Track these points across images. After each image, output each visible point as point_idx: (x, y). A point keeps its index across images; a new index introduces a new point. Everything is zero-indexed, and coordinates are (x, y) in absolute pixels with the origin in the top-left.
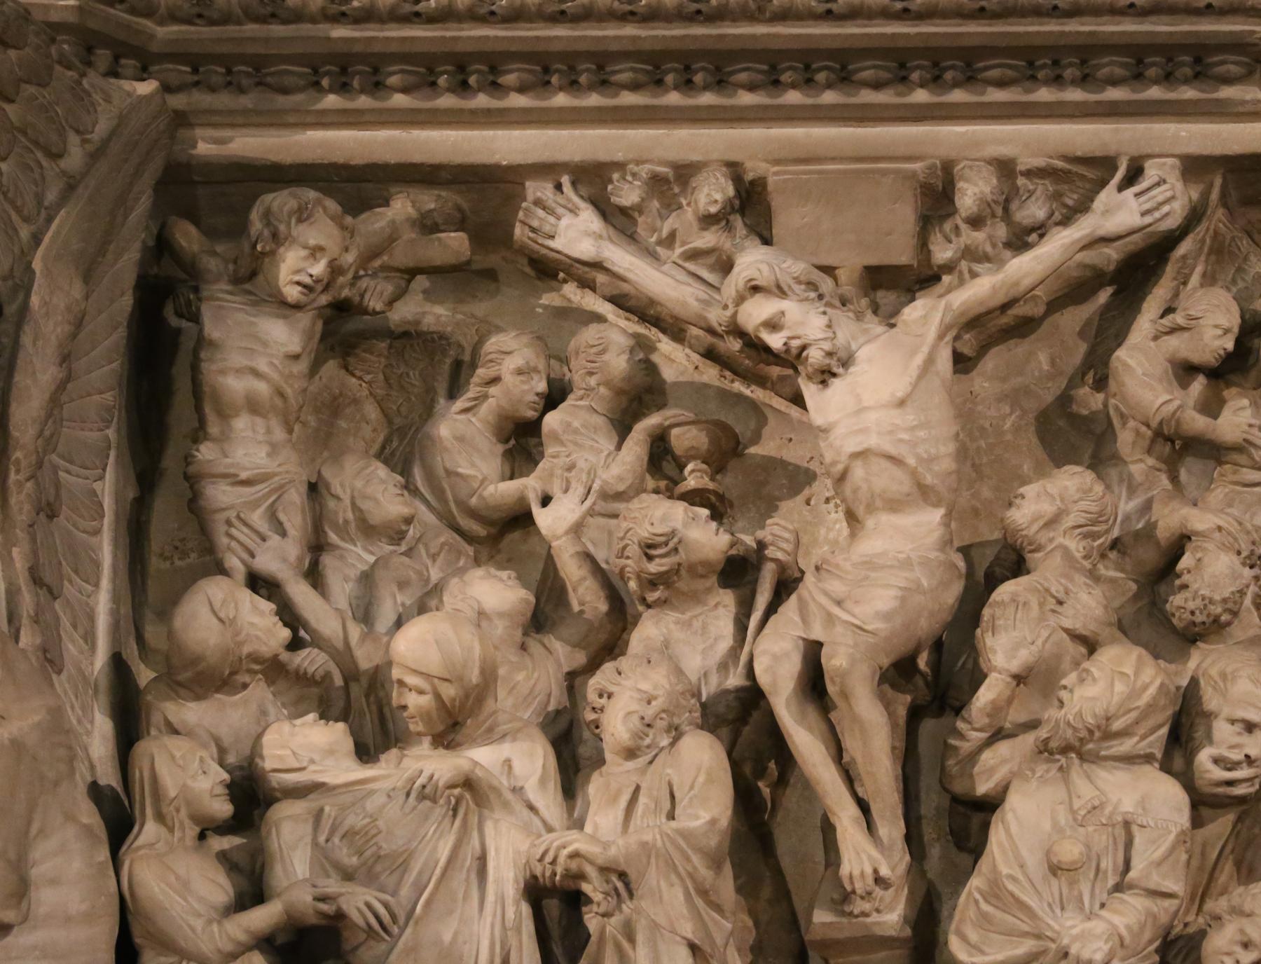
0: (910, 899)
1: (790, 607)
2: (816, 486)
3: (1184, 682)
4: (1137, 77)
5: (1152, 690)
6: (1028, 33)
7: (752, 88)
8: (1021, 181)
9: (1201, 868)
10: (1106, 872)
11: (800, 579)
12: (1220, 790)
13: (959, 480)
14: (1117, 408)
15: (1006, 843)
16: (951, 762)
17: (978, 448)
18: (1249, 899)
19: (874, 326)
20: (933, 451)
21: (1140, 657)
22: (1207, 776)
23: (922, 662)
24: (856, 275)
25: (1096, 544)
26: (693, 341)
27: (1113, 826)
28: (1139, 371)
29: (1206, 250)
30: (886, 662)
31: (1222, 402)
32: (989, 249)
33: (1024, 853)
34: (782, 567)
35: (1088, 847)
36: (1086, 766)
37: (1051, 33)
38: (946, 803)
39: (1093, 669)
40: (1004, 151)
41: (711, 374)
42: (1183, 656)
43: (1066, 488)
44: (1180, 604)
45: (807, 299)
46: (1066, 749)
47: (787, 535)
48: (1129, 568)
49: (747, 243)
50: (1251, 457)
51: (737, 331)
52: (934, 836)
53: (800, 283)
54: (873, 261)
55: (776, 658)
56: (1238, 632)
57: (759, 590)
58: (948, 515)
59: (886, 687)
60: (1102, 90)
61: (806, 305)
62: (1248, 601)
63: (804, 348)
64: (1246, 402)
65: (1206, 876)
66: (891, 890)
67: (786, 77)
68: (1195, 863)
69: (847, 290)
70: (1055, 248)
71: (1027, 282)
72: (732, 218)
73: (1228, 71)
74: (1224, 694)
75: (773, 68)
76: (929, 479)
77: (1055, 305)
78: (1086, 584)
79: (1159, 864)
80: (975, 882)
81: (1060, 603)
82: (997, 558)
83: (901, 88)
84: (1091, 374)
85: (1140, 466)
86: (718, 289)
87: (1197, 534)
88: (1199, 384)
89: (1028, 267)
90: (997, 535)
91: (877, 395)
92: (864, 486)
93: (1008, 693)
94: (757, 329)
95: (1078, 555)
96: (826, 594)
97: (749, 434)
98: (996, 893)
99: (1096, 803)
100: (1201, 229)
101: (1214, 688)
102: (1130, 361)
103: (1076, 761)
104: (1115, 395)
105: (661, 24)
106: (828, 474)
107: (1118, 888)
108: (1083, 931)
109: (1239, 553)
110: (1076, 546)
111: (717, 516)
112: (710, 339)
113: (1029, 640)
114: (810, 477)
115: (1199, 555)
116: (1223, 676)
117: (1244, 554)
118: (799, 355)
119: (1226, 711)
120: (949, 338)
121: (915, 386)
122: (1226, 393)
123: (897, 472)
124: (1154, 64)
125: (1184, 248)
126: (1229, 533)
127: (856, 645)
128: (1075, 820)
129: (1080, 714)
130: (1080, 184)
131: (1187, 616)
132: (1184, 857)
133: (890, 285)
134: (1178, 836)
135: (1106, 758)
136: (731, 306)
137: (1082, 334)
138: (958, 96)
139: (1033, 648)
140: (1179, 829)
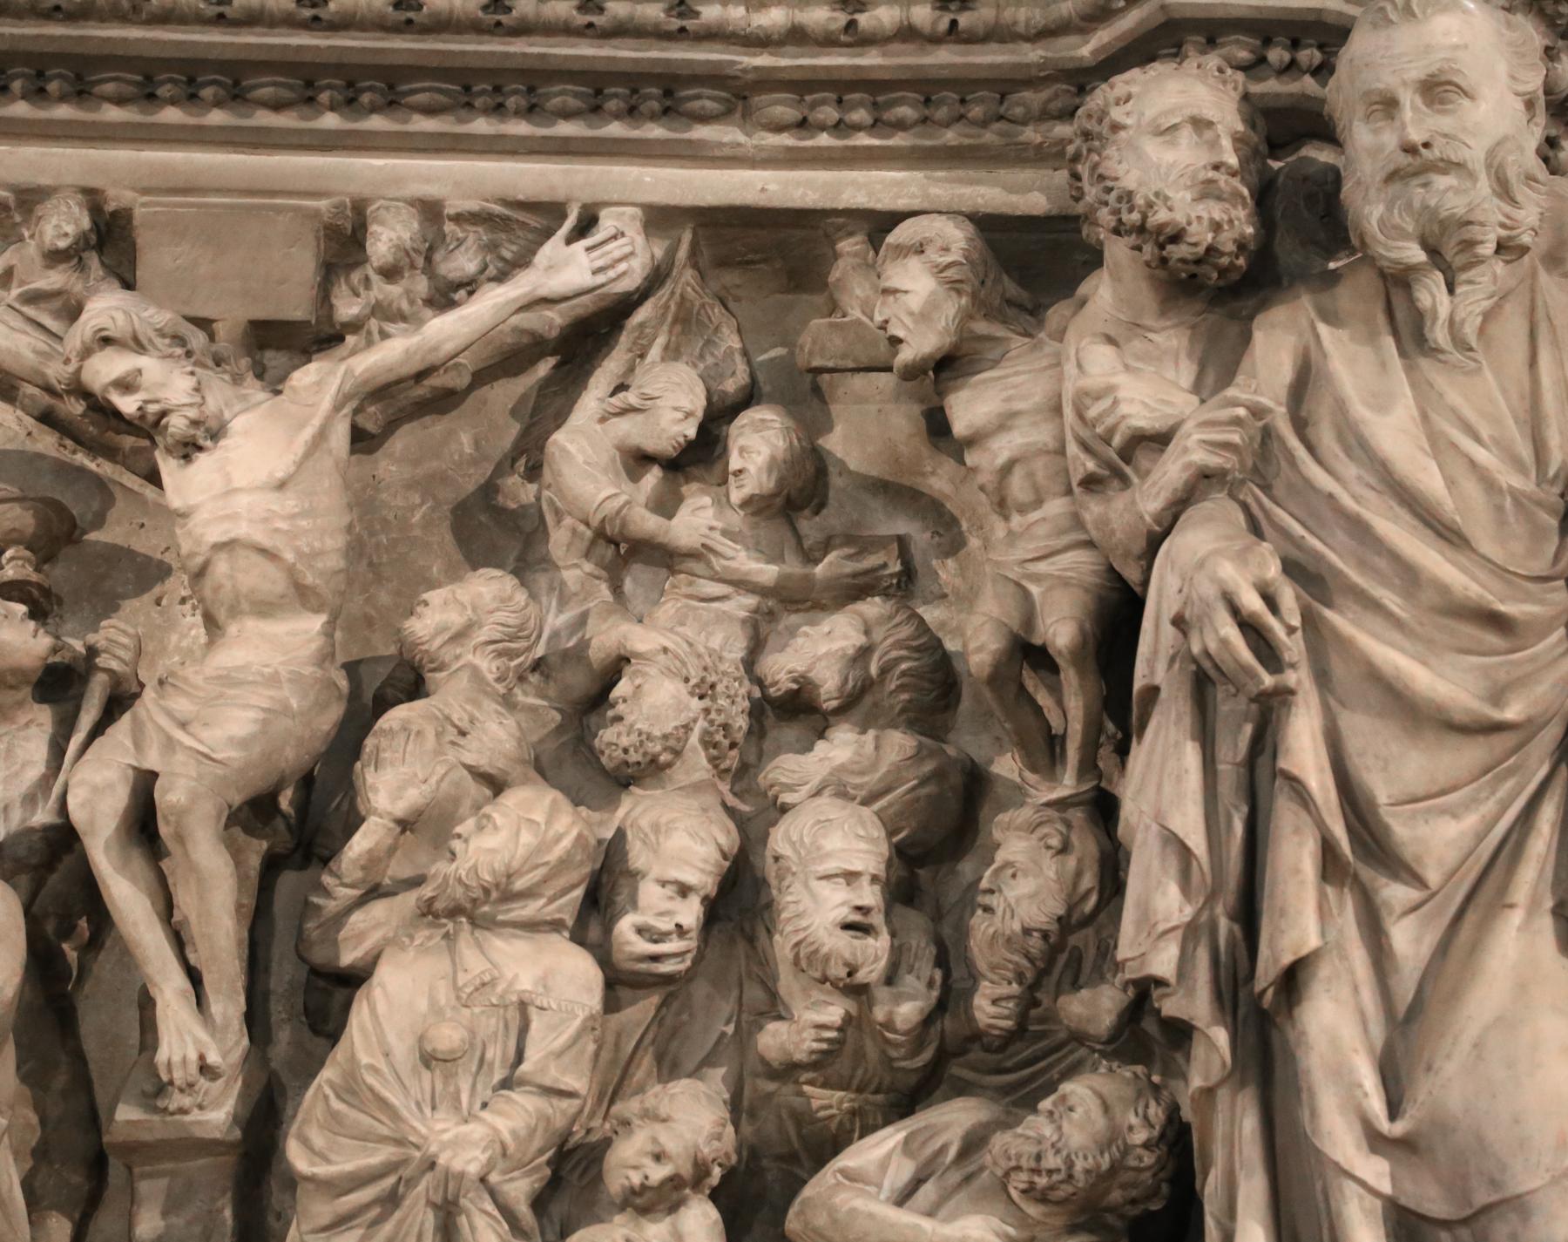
0: (243, 1096)
1: (121, 729)
2: (170, 583)
3: (609, 834)
4: (595, 110)
5: (566, 843)
6: (463, 53)
7: (120, 101)
8: (449, 227)
9: (613, 1062)
10: (491, 1064)
11: (137, 696)
12: (643, 966)
13: (350, 582)
14: (551, 502)
15: (369, 1026)
16: (310, 925)
17: (378, 545)
18: (666, 1100)
19: (255, 391)
20: (317, 544)
21: (554, 801)
22: (628, 948)
23: (285, 801)
24: (240, 330)
25: (513, 664)
26: (26, 401)
27: (506, 1007)
28: (580, 459)
29: (670, 319)
30: (237, 799)
31: (679, 499)
32: (405, 306)
33: (392, 1038)
34: (116, 679)
35: (472, 1033)
36: (478, 933)
37: (492, 53)
38: (303, 973)
39: (495, 815)
41: (47, 443)
42: (611, 803)
43: (480, 595)
44: (613, 739)
45: (171, 356)
46: (454, 912)
47: (125, 640)
48: (552, 693)
49: (104, 286)
50: (709, 564)
51: (80, 390)
52: (284, 1016)
53: (163, 336)
54: (261, 314)
55: (95, 789)
56: (681, 775)
57: (84, 707)
58: (331, 625)
59: (237, 831)
60: (553, 124)
61: (169, 363)
62: (694, 739)
63: (164, 414)
64: (707, 500)
65: (619, 1072)
66: (220, 1082)
67: (164, 91)
68: (605, 1055)
69: (222, 346)
70: (487, 308)
71: (449, 347)
72: (85, 255)
73: (703, 108)
75: (149, 78)
76: (309, 579)
77: (483, 377)
78: (497, 712)
79: (559, 1054)
80: (327, 1074)
81: (463, 734)
82: (390, 677)
83: (306, 110)
84: (523, 461)
85: (575, 572)
86: (59, 338)
87: (638, 655)
88: (653, 477)
89: (449, 330)
90: (392, 650)
91: (252, 476)
92: (228, 585)
93: (390, 841)
94: (105, 388)
95: (490, 677)
96: (169, 714)
97: (89, 516)
98: (351, 1089)
99: (487, 978)
100: (663, 294)
101: (644, 842)
102: (572, 448)
103: (466, 927)
104: (549, 486)
105: (9, 20)
106: (183, 568)
107: (506, 1084)
108: (456, 1137)
109: (687, 680)
110: (488, 666)
111: (38, 613)
112: (47, 399)
113: (421, 776)
114: (164, 571)
115: (637, 682)
116: (656, 828)
117: (693, 681)
118: (157, 423)
119: (656, 871)
120: (347, 410)
121: (300, 465)
122: (684, 489)
123: (271, 569)
124: (616, 95)
125: (642, 314)
126: (677, 657)
127: (200, 777)
128: (458, 998)
129: (475, 868)
130: (520, 233)
131: (619, 753)
132: (591, 1047)
133: (277, 344)
134: (585, 1020)
135: (505, 924)
136: (74, 360)
137: (514, 413)
138: (377, 123)
139: (424, 787)
140: (587, 1013)
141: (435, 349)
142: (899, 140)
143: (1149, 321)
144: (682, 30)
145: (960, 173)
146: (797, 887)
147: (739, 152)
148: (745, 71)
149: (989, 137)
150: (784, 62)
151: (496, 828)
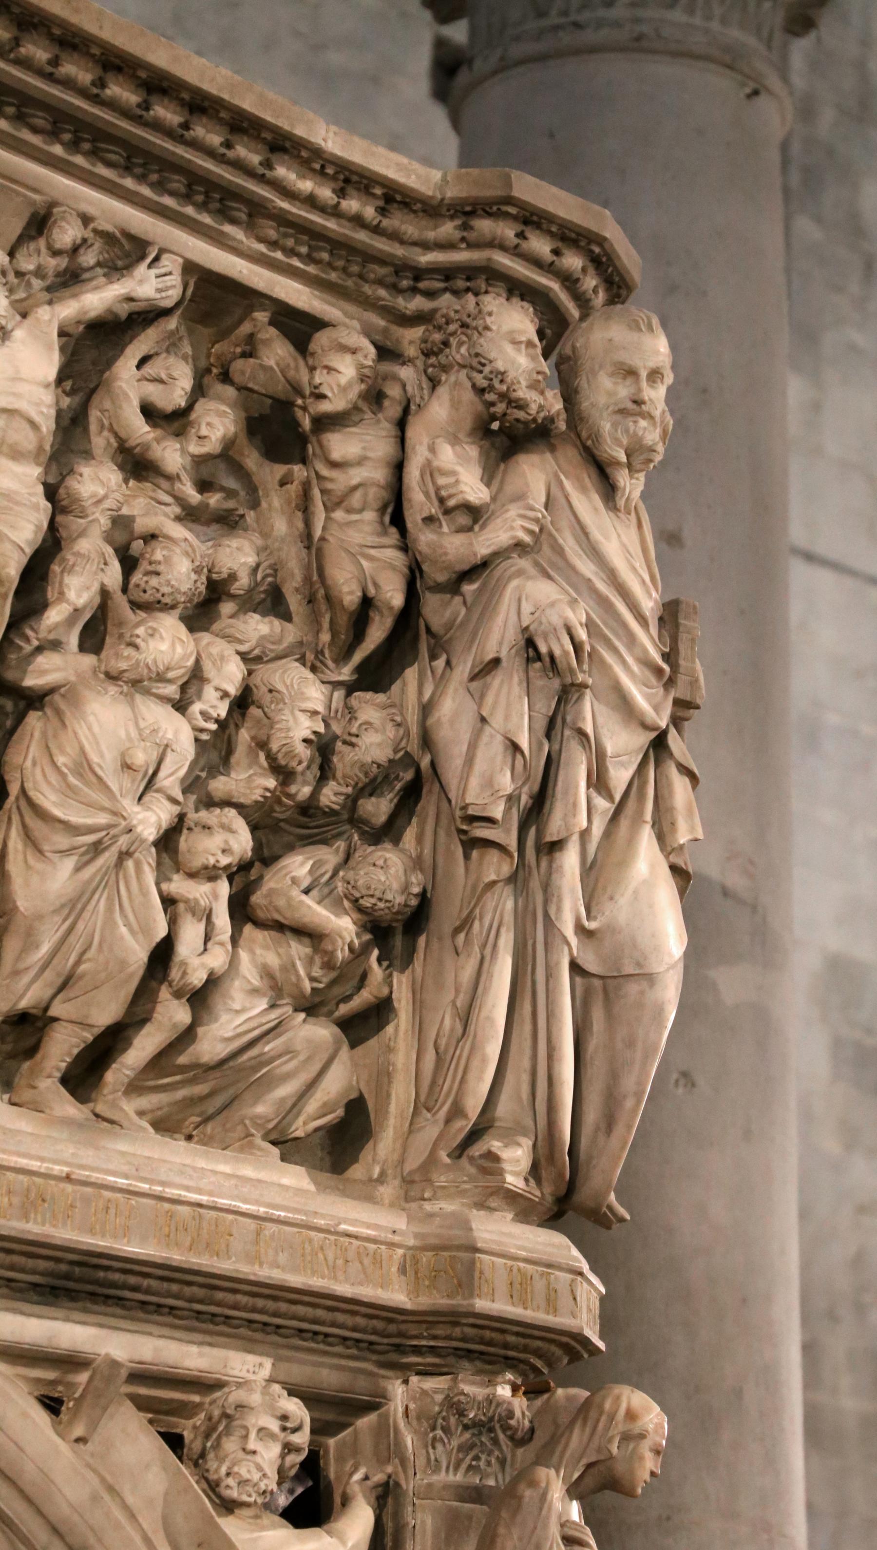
4: (187, 197)
33: (104, 747)
40: (91, 210)
74: (219, 670)
119: (216, 682)
141: (85, 313)
142: (311, 269)
143: (461, 436)
144: (263, 175)
145: (325, 296)
146: (287, 711)
147: (240, 246)
148: (274, 208)
149: (349, 283)
150: (294, 210)
151: (162, 638)
